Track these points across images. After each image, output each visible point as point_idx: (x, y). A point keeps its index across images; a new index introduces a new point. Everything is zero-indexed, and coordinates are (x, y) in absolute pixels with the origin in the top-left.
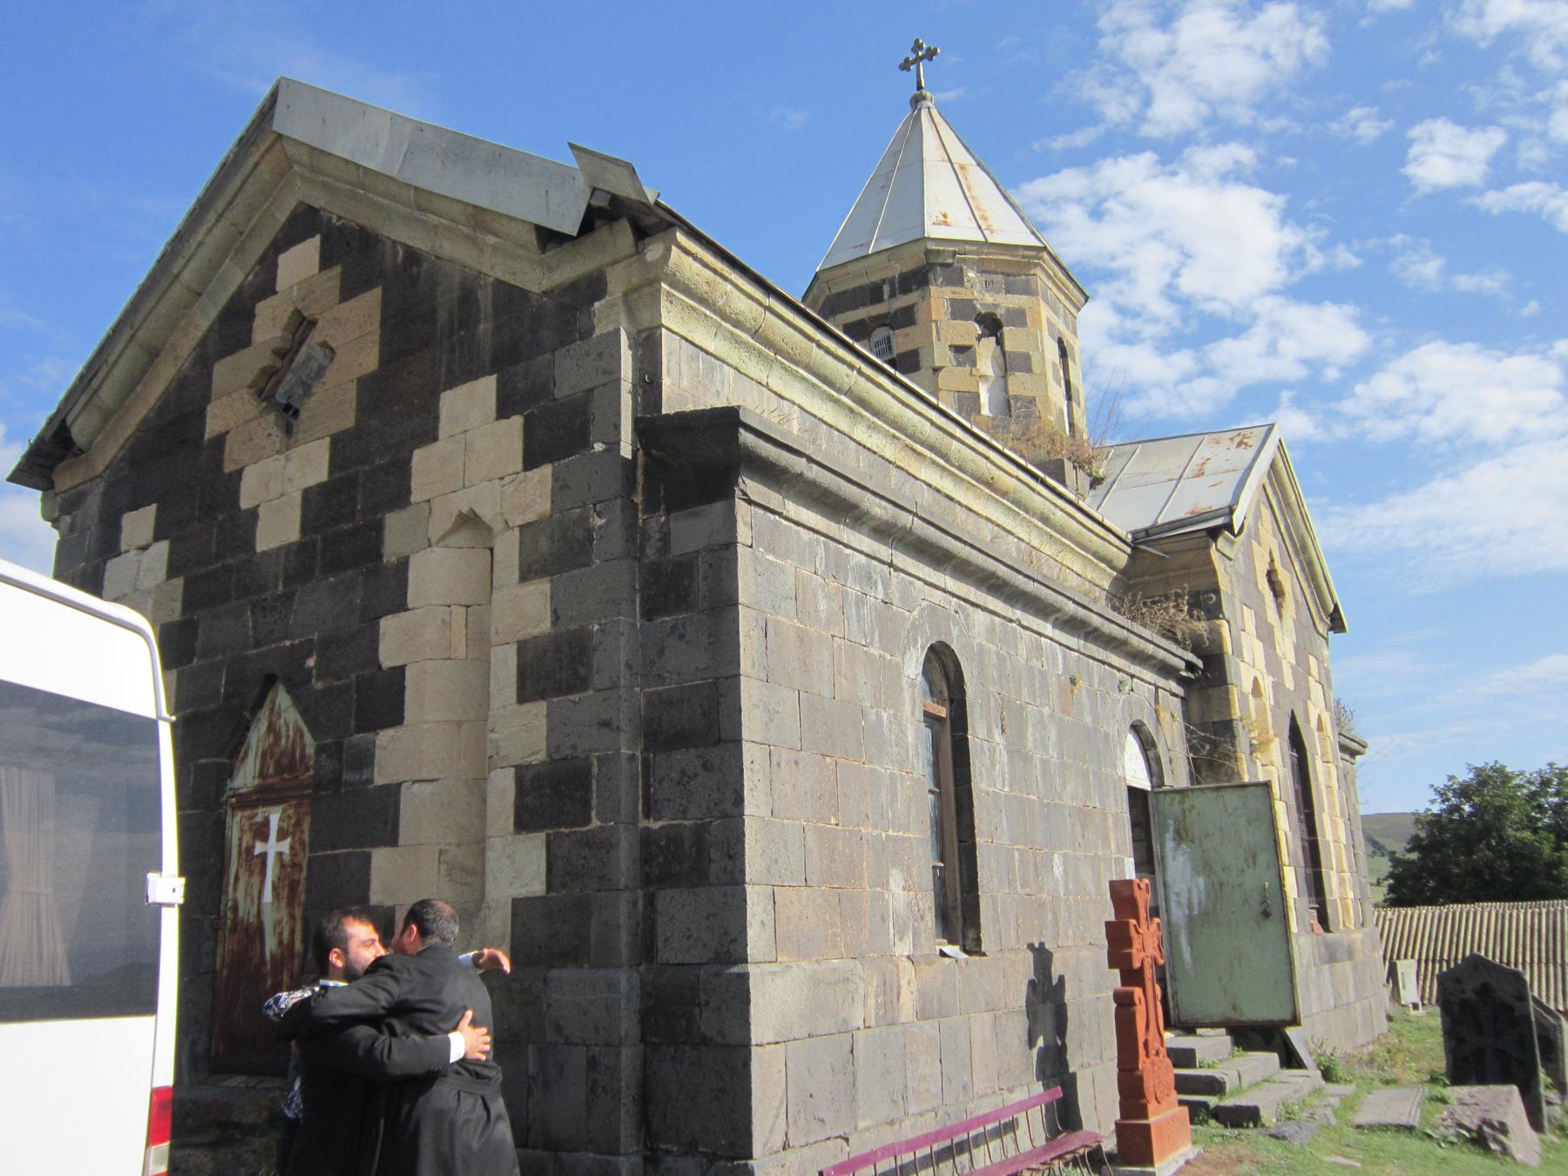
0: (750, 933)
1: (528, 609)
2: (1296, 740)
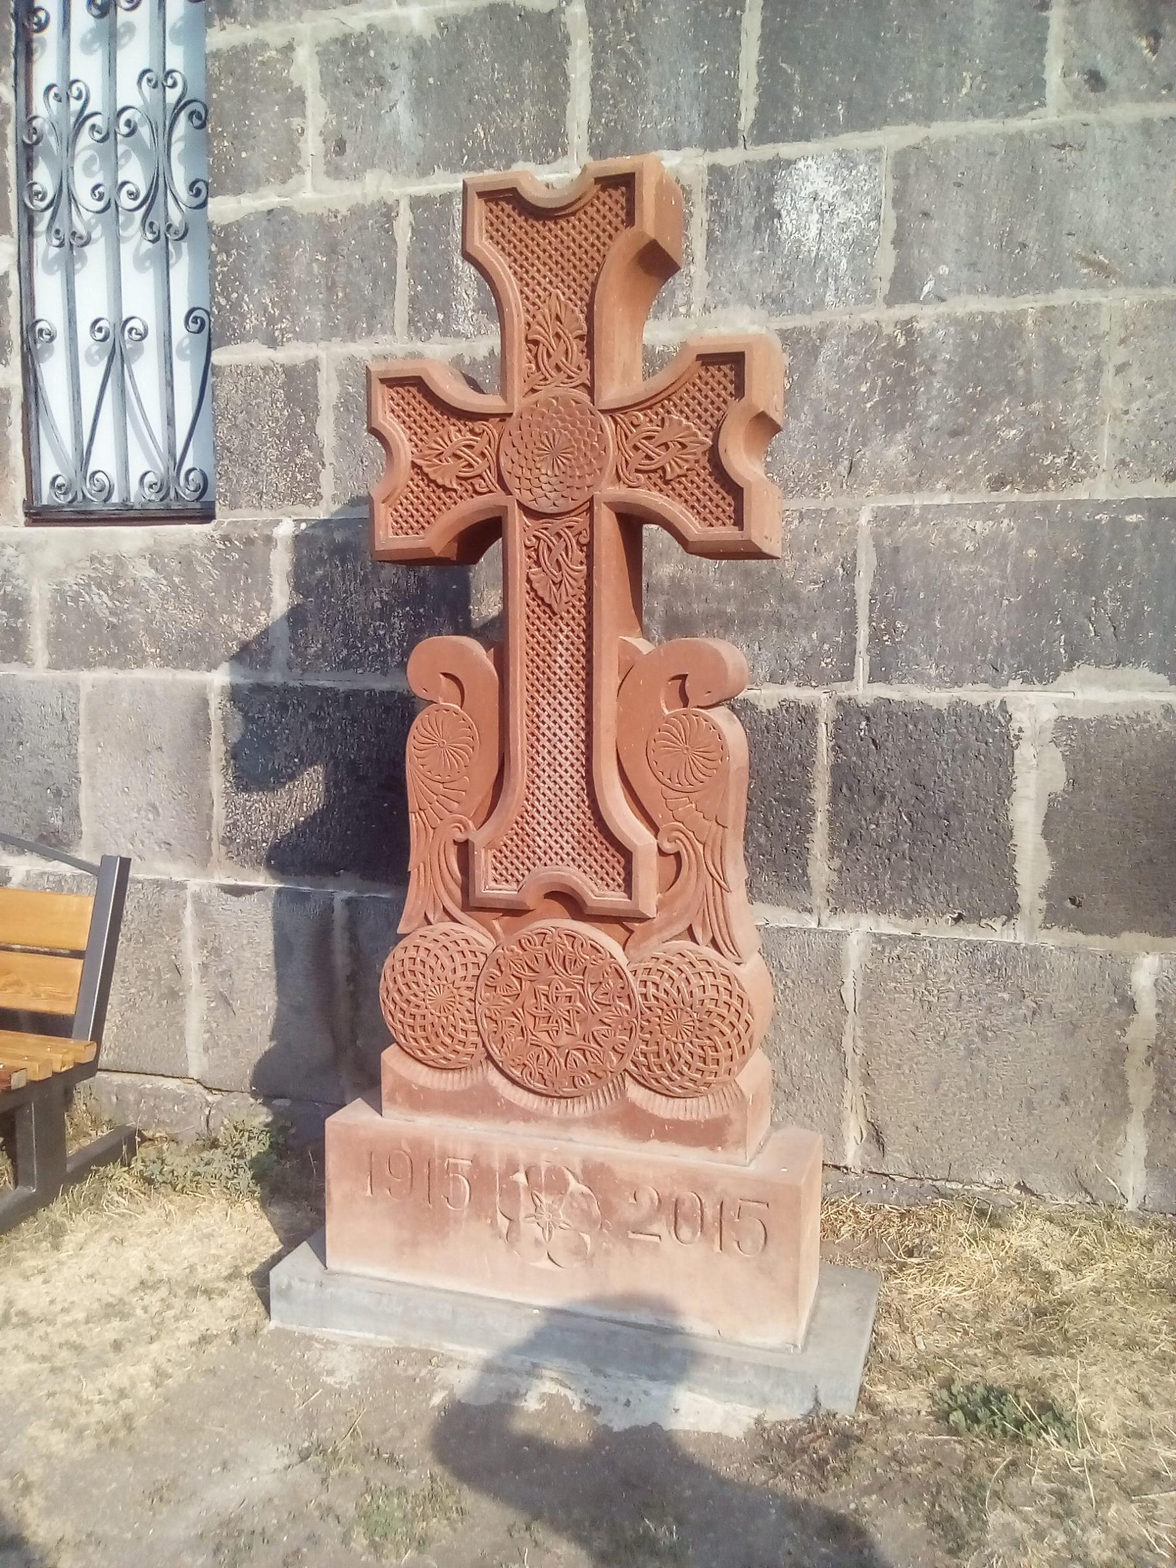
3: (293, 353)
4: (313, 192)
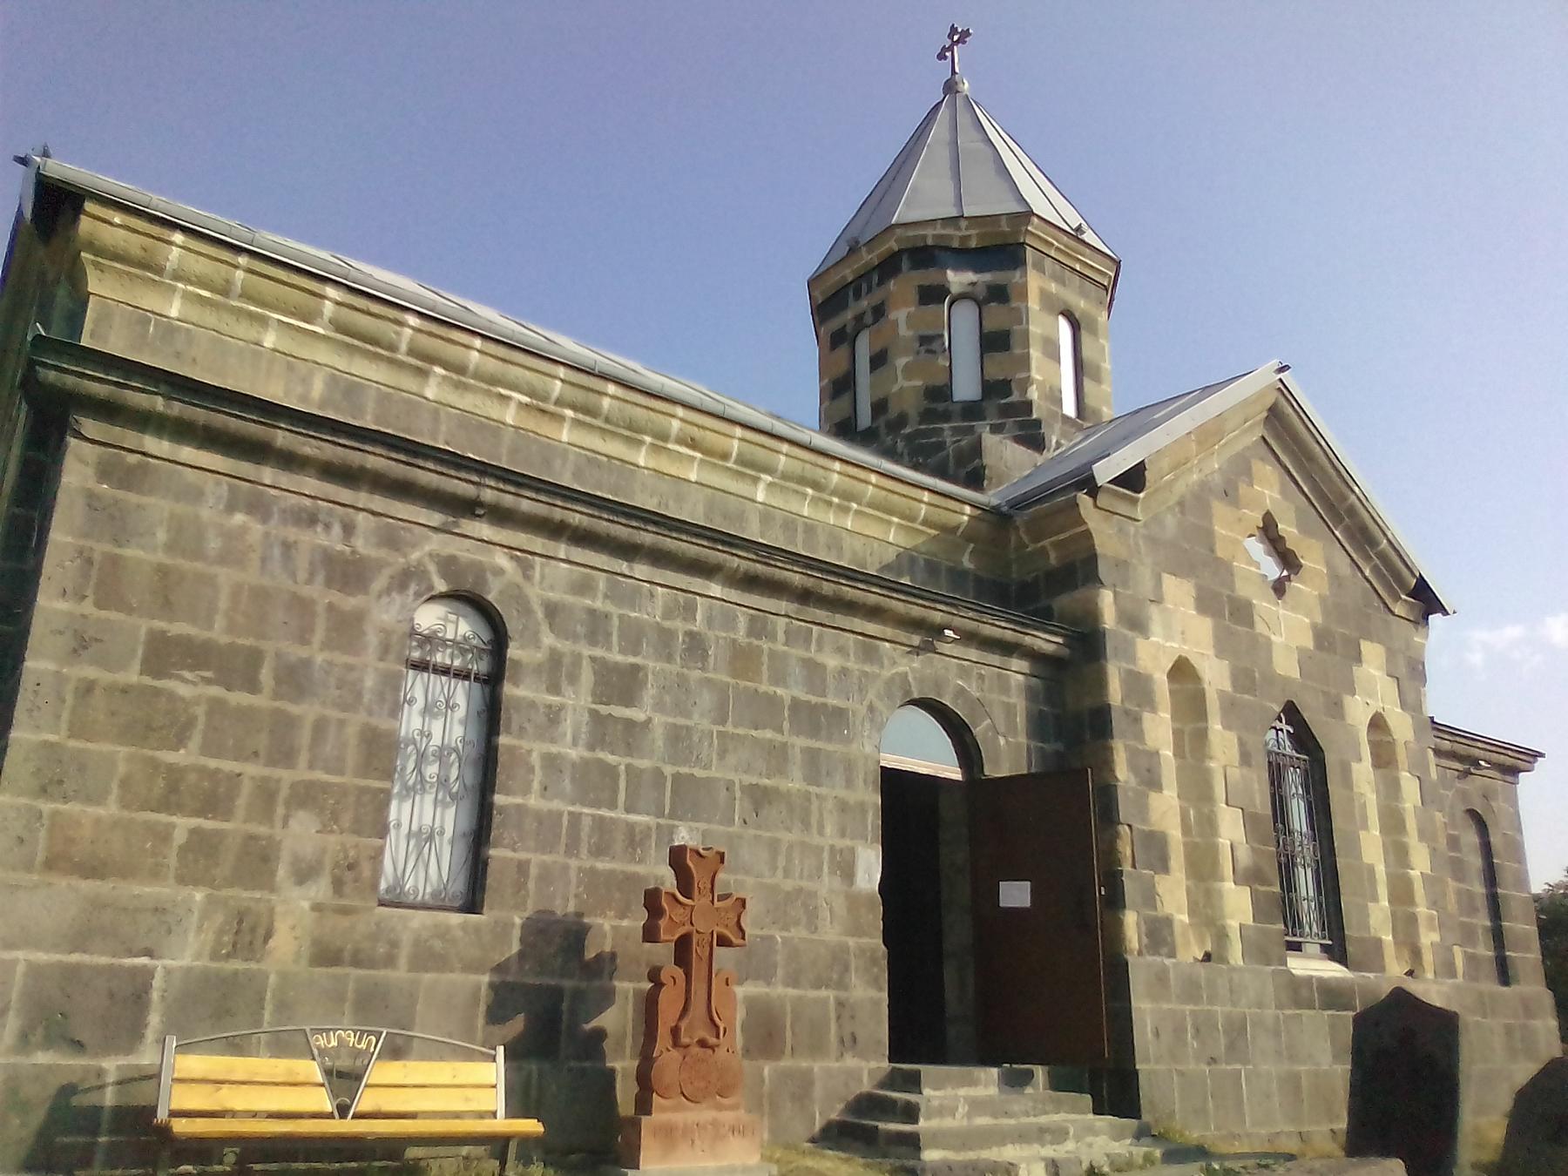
3: (522, 855)
4: (534, 801)
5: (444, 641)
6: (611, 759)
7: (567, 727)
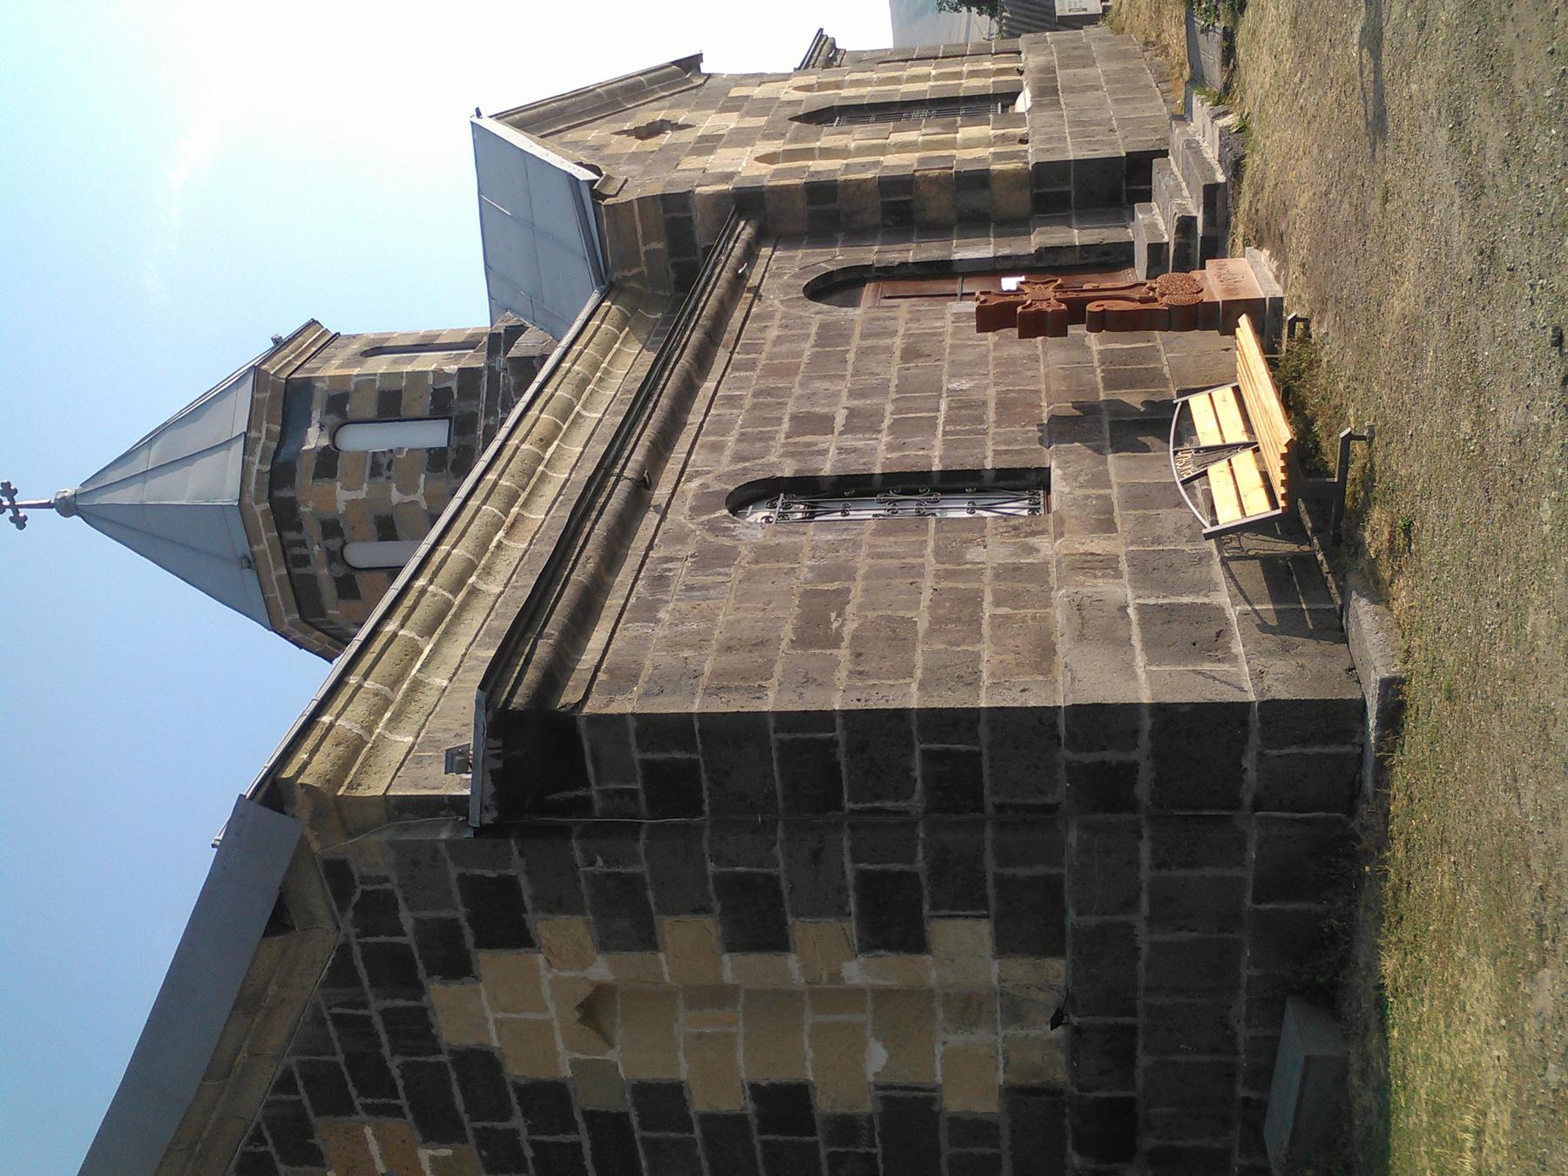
0: (1032, 704)
1: (689, 943)
2: (821, 117)
3: (990, 454)
5: (782, 516)
6: (887, 422)
7: (859, 444)
